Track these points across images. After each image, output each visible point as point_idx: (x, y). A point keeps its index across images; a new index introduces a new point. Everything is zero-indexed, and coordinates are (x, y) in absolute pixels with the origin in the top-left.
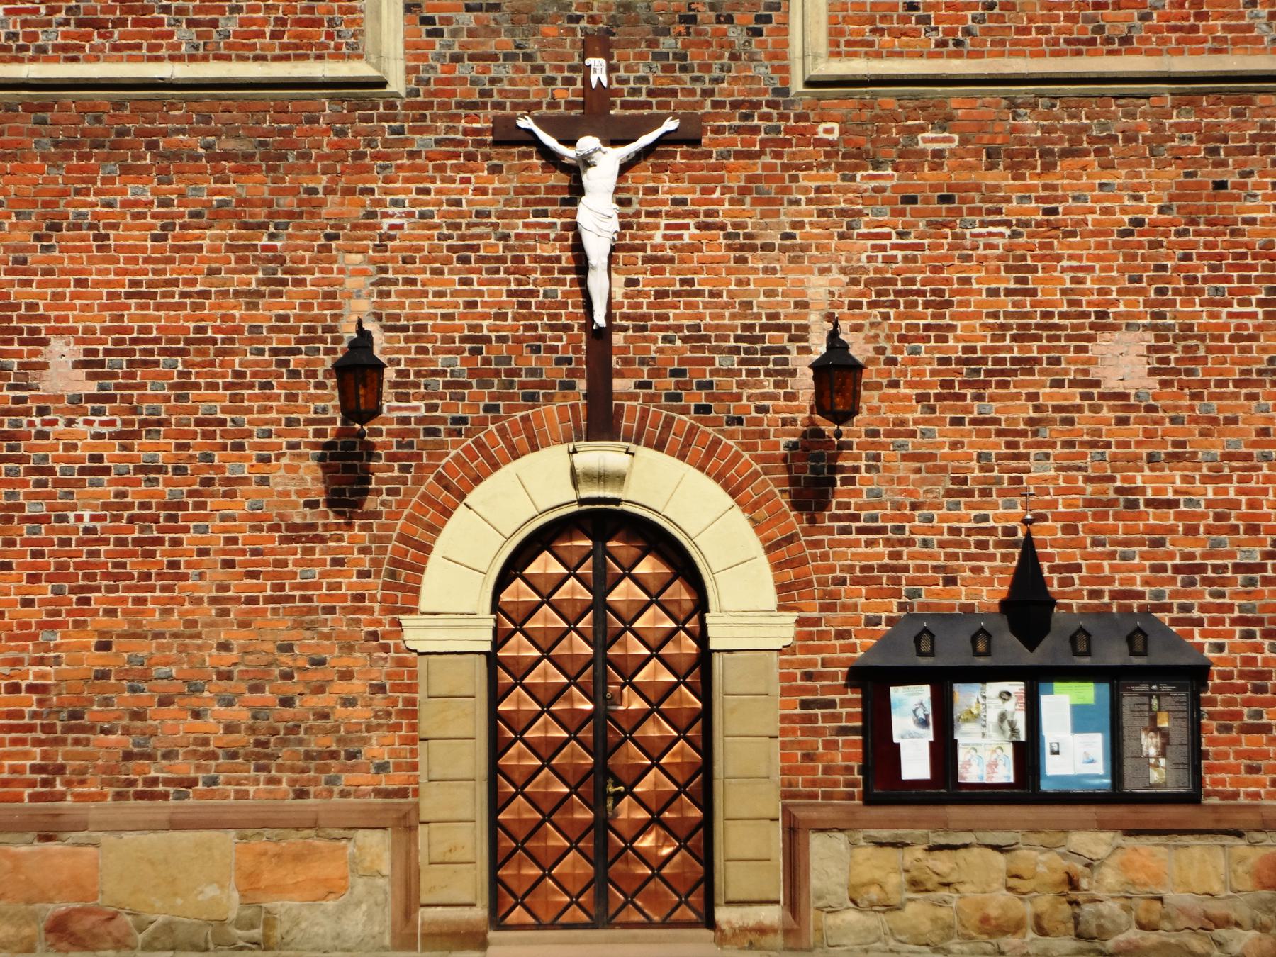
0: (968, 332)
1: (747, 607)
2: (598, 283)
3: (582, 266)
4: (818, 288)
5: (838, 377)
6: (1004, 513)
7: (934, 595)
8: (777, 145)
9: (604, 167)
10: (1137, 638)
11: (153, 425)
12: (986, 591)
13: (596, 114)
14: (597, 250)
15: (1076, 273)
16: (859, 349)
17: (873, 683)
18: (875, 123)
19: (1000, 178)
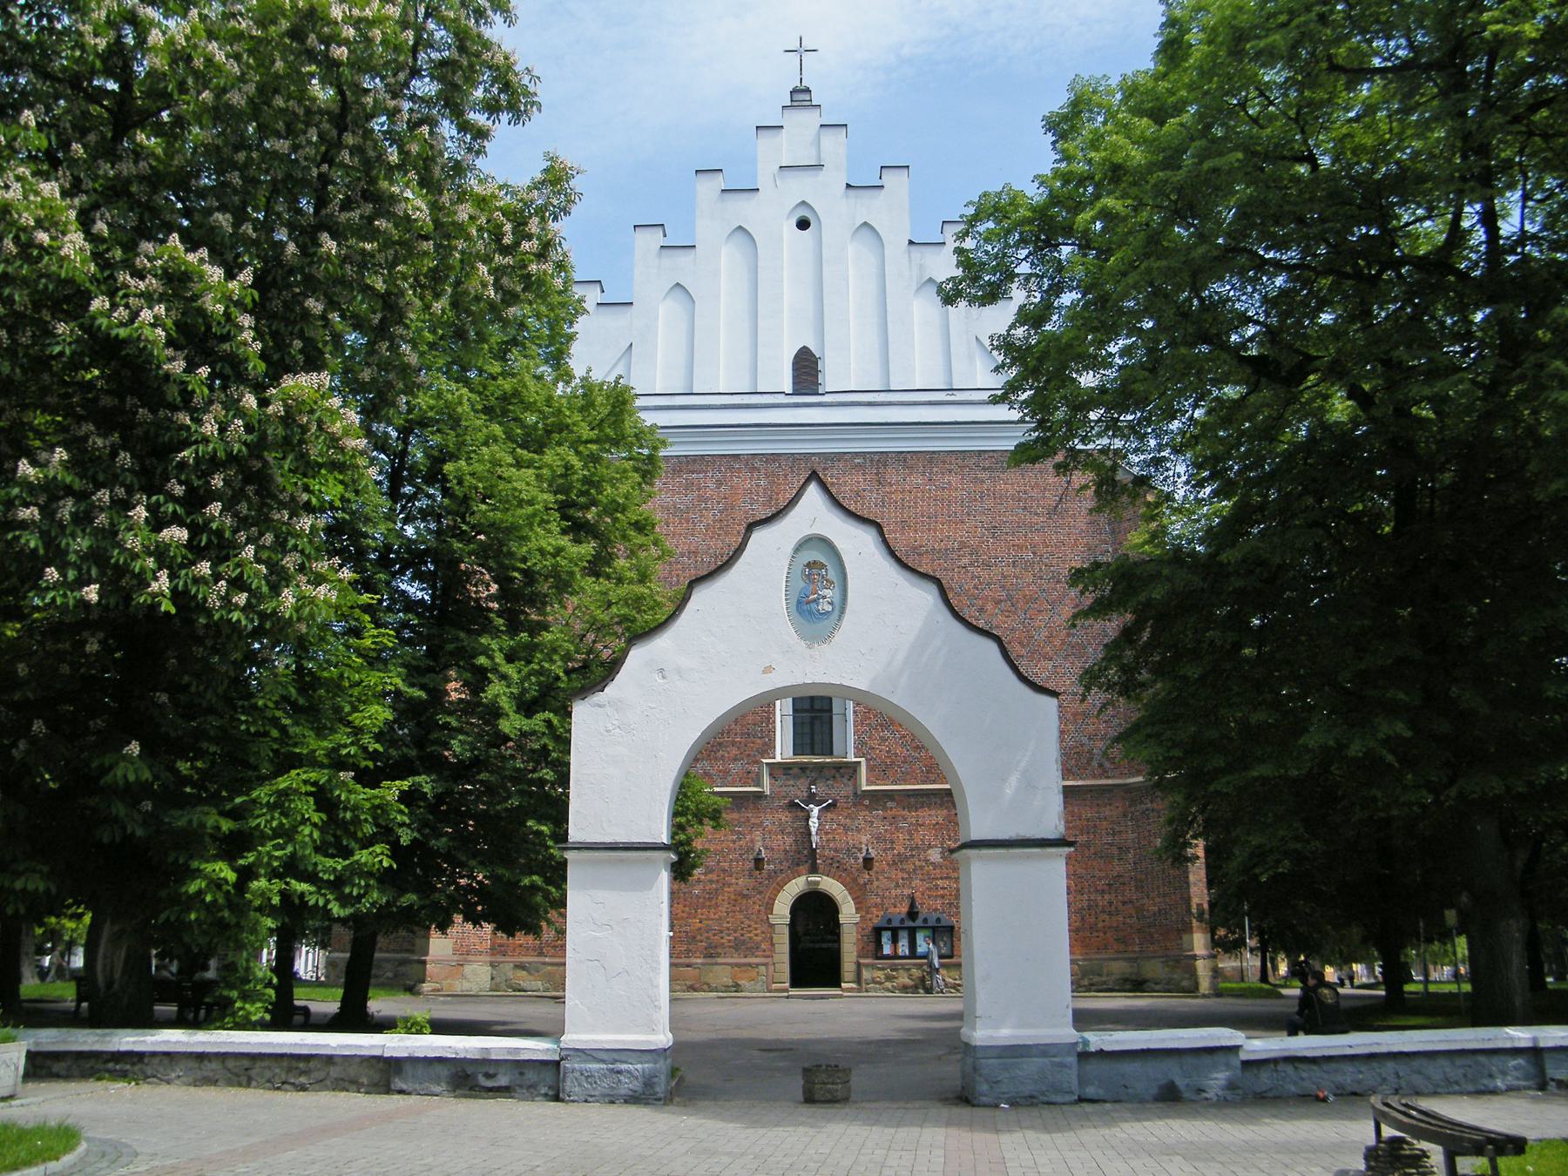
0: (899, 849)
1: (848, 913)
2: (815, 839)
3: (810, 834)
4: (864, 839)
5: (868, 862)
6: (907, 892)
7: (892, 910)
8: (855, 805)
9: (816, 810)
10: (938, 920)
11: (712, 871)
12: (904, 909)
13: (811, 798)
14: (814, 830)
15: (924, 835)
16: (873, 853)
17: (878, 931)
18: (878, 799)
19: (905, 812)
